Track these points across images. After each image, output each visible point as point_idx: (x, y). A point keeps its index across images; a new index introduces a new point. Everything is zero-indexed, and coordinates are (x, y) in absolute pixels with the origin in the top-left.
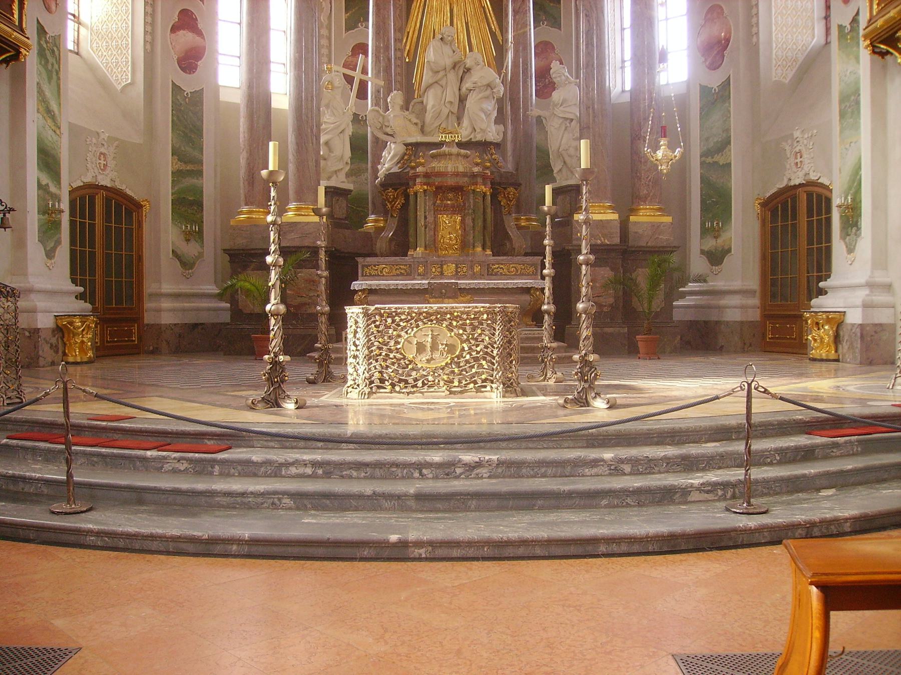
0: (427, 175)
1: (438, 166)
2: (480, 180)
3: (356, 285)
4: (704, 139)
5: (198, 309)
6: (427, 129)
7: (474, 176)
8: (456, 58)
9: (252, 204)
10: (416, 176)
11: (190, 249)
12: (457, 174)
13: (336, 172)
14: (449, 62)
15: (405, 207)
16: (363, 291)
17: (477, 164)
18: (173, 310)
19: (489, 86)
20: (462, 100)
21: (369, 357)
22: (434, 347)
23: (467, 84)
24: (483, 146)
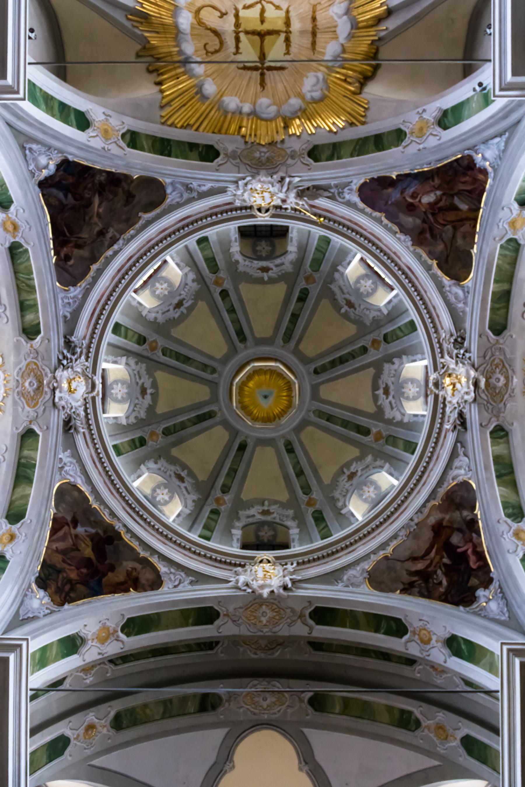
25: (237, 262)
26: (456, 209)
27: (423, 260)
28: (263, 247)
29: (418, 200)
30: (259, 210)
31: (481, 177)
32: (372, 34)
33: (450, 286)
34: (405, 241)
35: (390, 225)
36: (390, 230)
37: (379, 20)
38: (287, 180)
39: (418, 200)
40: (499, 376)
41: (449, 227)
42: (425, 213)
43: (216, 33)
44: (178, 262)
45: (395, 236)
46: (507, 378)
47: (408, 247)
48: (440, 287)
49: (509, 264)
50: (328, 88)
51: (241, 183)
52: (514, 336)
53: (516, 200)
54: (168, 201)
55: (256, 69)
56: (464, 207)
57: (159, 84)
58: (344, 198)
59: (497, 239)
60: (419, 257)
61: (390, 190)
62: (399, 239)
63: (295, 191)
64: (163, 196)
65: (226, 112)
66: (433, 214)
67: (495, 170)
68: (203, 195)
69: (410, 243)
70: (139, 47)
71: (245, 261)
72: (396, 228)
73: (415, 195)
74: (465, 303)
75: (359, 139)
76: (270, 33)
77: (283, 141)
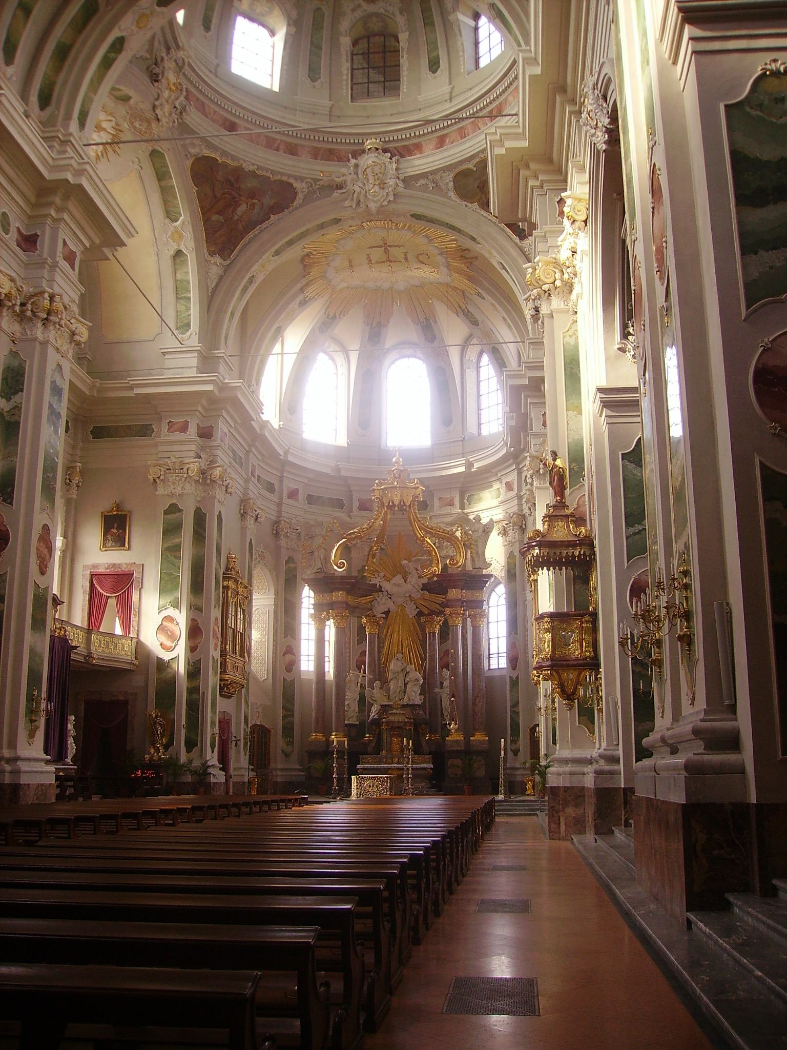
0: (387, 722)
1: (391, 718)
2: (408, 724)
3: (359, 766)
4: (511, 700)
5: (291, 775)
6: (391, 698)
7: (406, 722)
8: (403, 668)
9: (317, 732)
10: (383, 723)
11: (289, 749)
12: (398, 722)
13: (352, 717)
14: (400, 669)
15: (379, 733)
16: (361, 769)
17: (407, 718)
18: (282, 776)
19: (417, 680)
20: (406, 684)
21: (357, 788)
22: (373, 786)
23: (407, 679)
24: (413, 707)
25: (401, 13)
26: (219, 213)
27: (230, 158)
28: (375, 25)
29: (249, 204)
30: (377, 149)
31: (212, 249)
32: (308, 278)
33: (202, 150)
34: (249, 165)
35: (264, 173)
36: (262, 169)
37: (307, 285)
38: (354, 207)
39: (249, 204)
40: (140, 127)
41: (219, 195)
42: (240, 196)
43: (423, 263)
44: (458, 34)
45: (257, 165)
46: (135, 127)
47: (245, 161)
48: (210, 146)
49: (169, 201)
50: (334, 246)
51: (392, 199)
52: (141, 152)
53: (187, 256)
54: (452, 176)
55: (390, 246)
56: (215, 217)
57: (460, 246)
58: (306, 183)
59: (187, 223)
60: (234, 158)
61: (272, 202)
62: (253, 164)
63: (347, 188)
64: (455, 177)
65: (409, 228)
66: (234, 198)
67: (206, 261)
68: (424, 175)
69: (244, 165)
70: (476, 263)
71: (393, 14)
72: (259, 172)
73: (252, 207)
74: (184, 146)
75: (305, 237)
76: (384, 262)
77: (363, 223)
